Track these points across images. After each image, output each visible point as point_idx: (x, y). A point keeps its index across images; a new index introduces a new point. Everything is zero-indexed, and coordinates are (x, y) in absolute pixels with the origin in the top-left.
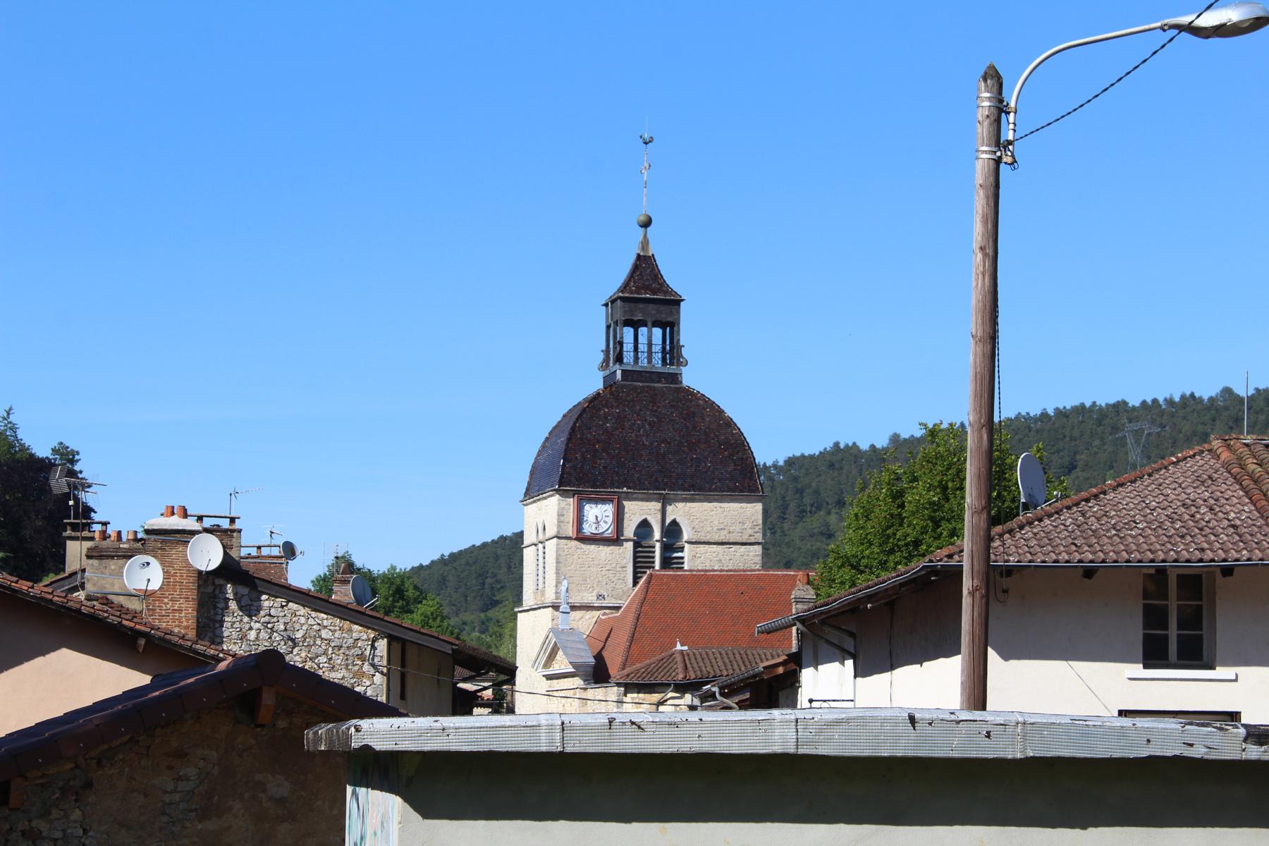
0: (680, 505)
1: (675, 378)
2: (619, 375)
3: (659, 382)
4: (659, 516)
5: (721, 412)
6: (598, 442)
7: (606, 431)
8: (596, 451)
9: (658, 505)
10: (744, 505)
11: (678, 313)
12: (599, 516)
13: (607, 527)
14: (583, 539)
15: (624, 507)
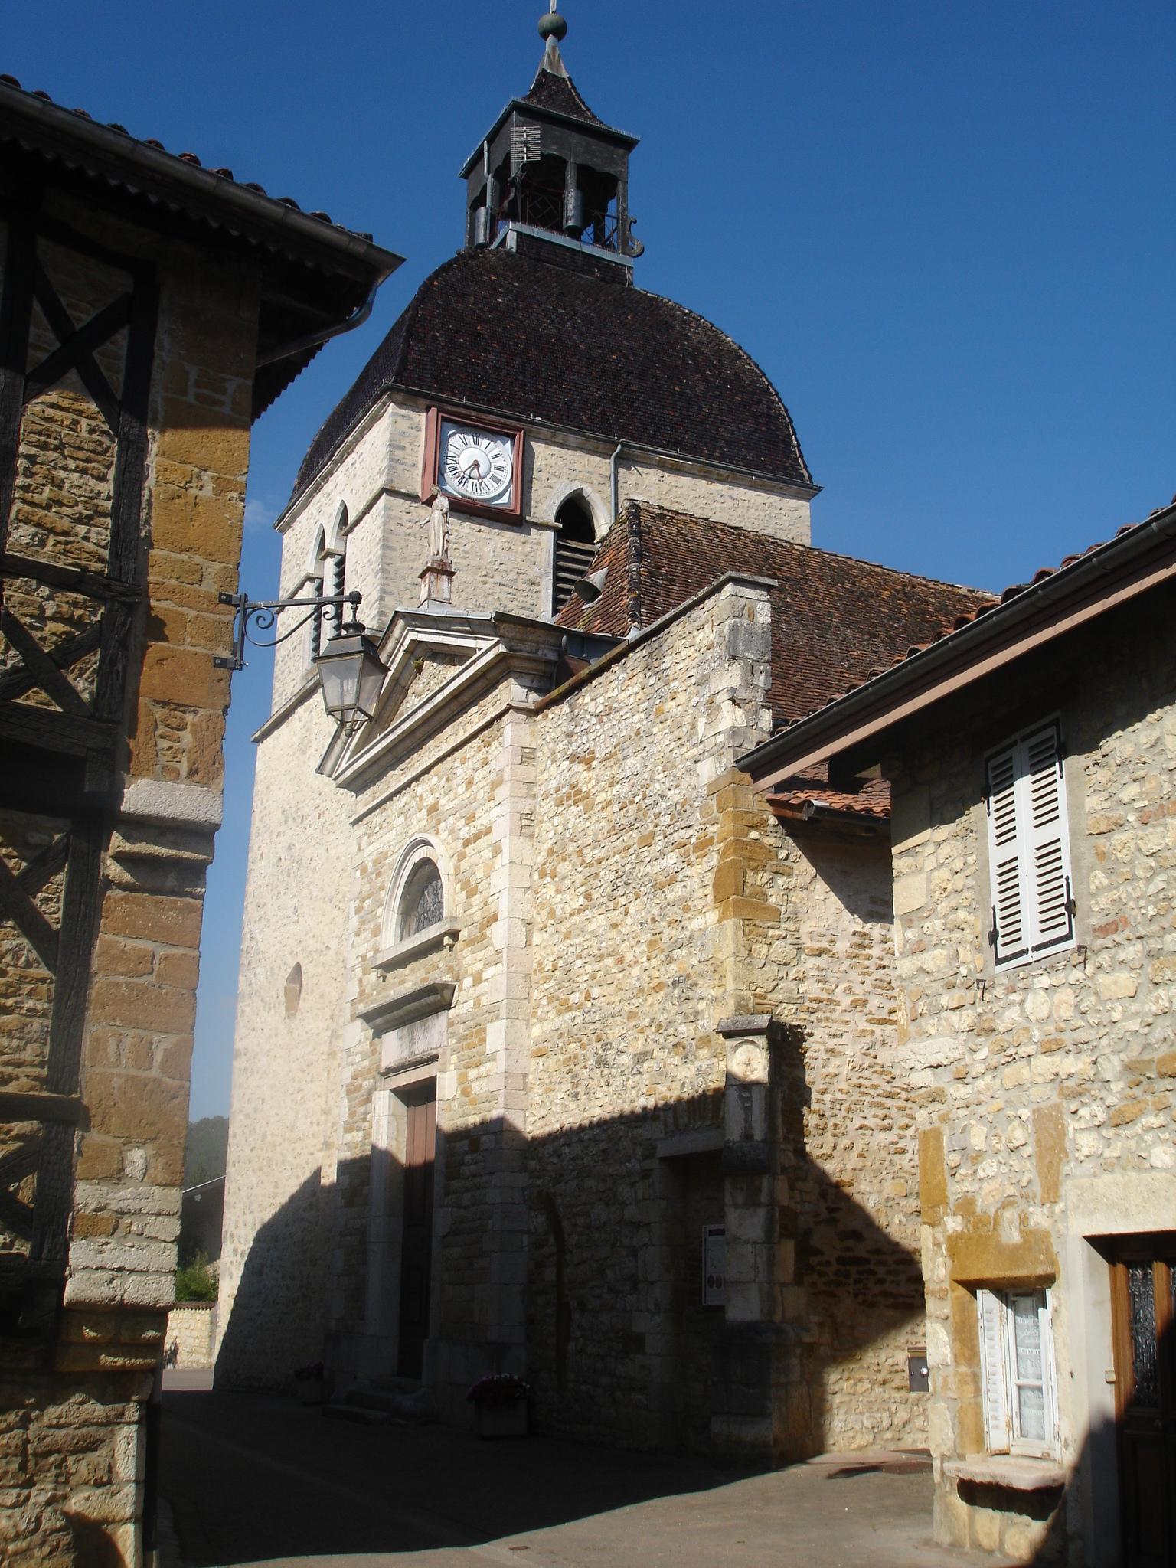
1: (615, 274)
2: (512, 243)
3: (591, 272)
4: (610, 491)
11: (625, 163)
12: (482, 462)
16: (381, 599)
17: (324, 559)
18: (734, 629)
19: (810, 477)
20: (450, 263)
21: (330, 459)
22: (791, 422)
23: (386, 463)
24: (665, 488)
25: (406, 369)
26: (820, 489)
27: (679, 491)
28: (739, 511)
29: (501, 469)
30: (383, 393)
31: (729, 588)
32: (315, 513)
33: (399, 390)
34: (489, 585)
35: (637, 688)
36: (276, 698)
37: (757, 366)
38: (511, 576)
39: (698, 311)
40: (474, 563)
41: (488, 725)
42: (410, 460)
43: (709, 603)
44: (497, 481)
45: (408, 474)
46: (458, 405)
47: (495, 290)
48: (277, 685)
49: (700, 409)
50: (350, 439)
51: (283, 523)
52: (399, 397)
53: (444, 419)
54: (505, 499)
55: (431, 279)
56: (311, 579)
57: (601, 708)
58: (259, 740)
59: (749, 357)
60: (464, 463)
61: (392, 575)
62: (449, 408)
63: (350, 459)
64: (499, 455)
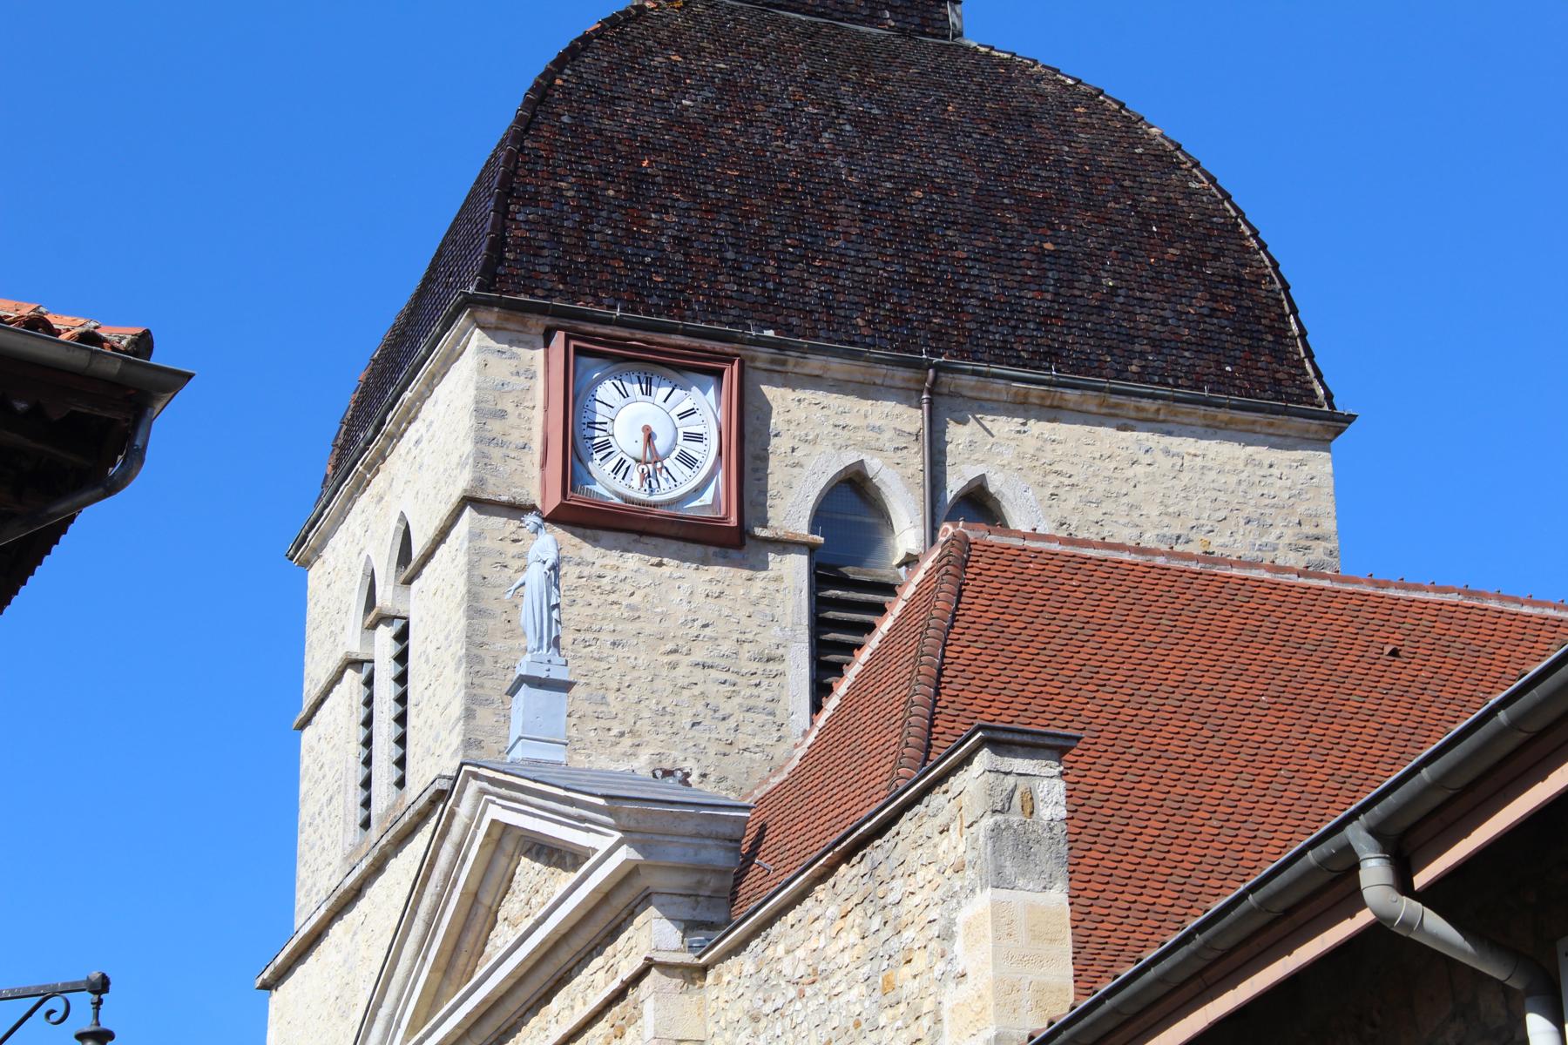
0: (1004, 426)
4: (917, 461)
5: (1131, 123)
6: (649, 148)
7: (678, 120)
8: (641, 178)
9: (913, 419)
10: (1262, 453)
12: (659, 430)
13: (693, 481)
14: (583, 517)
15: (766, 410)
16: (469, 714)
17: (373, 626)
18: (996, 832)
19: (1329, 396)
20: (586, 39)
21: (377, 430)
22: (1286, 287)
23: (468, 447)
24: (1029, 444)
25: (502, 259)
26: (1350, 419)
27: (1060, 449)
28: (1185, 478)
29: (698, 438)
30: (459, 310)
31: (984, 758)
32: (359, 531)
33: (489, 303)
34: (680, 671)
35: (852, 937)
36: (300, 896)
37: (1212, 180)
38: (726, 647)
39: (1092, 80)
40: (649, 629)
41: (619, 996)
42: (516, 438)
43: (955, 783)
44: (689, 461)
45: (513, 465)
46: (607, 322)
47: (677, 82)
48: (302, 872)
49: (1097, 281)
50: (407, 395)
51: (304, 547)
52: (491, 316)
53: (579, 352)
54: (708, 497)
55: (548, 75)
56: (355, 663)
57: (802, 970)
58: (269, 986)
59: (1197, 165)
60: (627, 440)
61: (489, 665)
62: (589, 328)
63: (412, 433)
64: (691, 412)
